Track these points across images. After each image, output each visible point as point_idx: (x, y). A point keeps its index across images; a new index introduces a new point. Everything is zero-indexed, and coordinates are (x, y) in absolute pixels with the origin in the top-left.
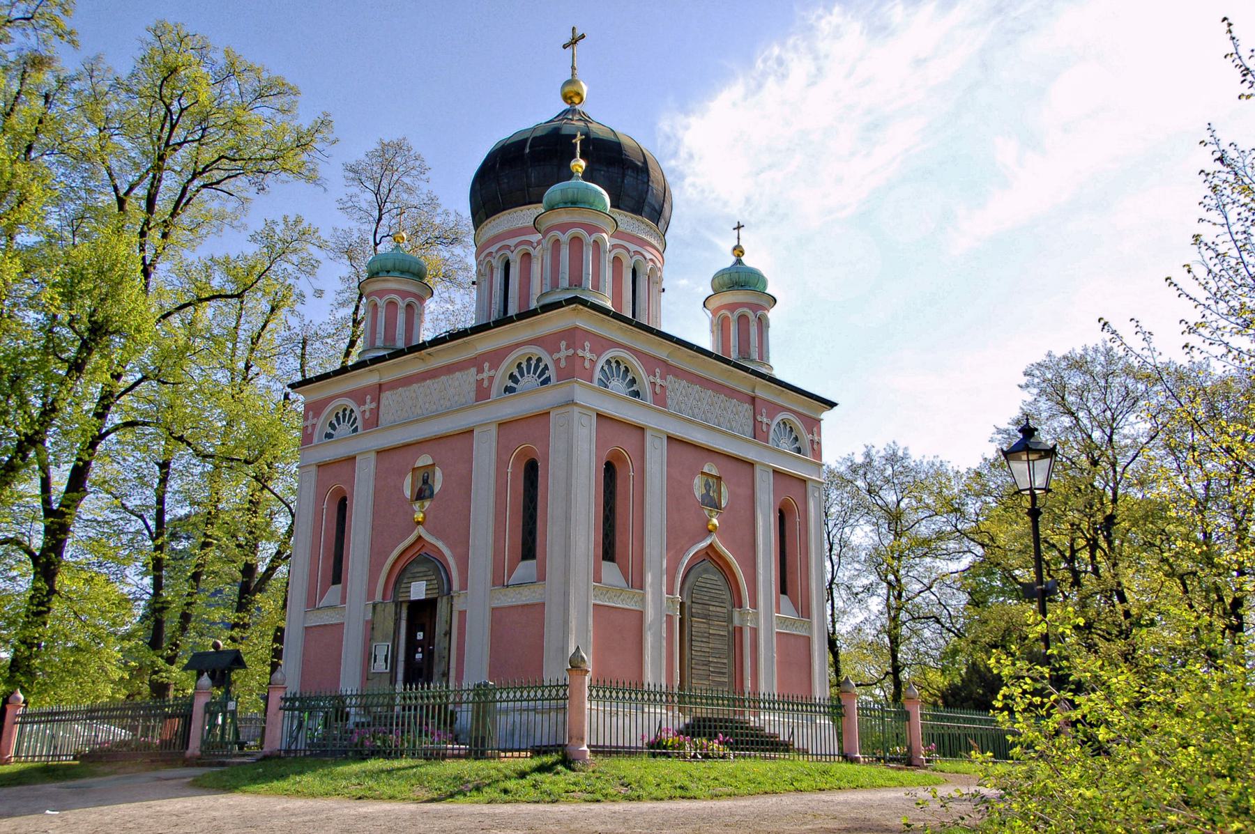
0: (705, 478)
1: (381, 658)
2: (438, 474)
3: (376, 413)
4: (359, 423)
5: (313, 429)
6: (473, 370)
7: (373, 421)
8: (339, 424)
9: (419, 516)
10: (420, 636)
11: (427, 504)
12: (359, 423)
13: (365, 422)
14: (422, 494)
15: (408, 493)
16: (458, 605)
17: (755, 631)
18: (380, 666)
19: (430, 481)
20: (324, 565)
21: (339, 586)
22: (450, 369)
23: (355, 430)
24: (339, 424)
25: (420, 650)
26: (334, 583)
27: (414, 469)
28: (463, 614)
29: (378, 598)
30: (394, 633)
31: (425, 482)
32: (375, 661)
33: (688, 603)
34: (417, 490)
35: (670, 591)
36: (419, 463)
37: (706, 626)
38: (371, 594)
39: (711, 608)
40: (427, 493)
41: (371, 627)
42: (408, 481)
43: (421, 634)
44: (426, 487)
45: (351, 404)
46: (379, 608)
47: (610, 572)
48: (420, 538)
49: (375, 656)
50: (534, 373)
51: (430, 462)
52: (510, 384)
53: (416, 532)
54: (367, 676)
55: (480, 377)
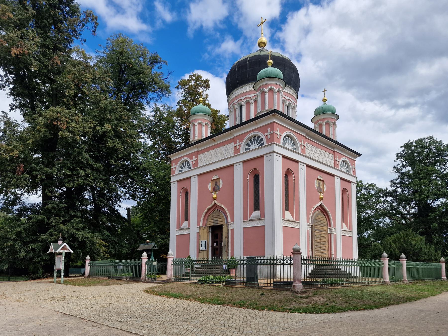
0: (318, 181)
1: (203, 245)
2: (221, 182)
3: (197, 161)
5: (175, 169)
8: (184, 167)
9: (215, 196)
11: (217, 193)
12: (191, 166)
13: (193, 164)
14: (215, 189)
15: (210, 189)
16: (231, 227)
17: (335, 235)
18: (203, 248)
19: (218, 184)
20: (182, 215)
21: (187, 222)
22: (223, 144)
23: (190, 168)
24: (184, 167)
26: (185, 221)
27: (212, 180)
28: (232, 230)
29: (201, 225)
30: (208, 236)
31: (216, 184)
32: (201, 247)
33: (314, 225)
34: (213, 188)
35: (308, 221)
36: (214, 178)
37: (319, 234)
38: (199, 224)
39: (321, 227)
40: (217, 188)
41: (199, 234)
42: (210, 185)
44: (217, 186)
45: (188, 159)
46: (202, 229)
47: (287, 213)
48: (215, 204)
49: (201, 245)
50: (257, 142)
51: (217, 177)
52: (247, 147)
53: (214, 202)
54: (199, 251)
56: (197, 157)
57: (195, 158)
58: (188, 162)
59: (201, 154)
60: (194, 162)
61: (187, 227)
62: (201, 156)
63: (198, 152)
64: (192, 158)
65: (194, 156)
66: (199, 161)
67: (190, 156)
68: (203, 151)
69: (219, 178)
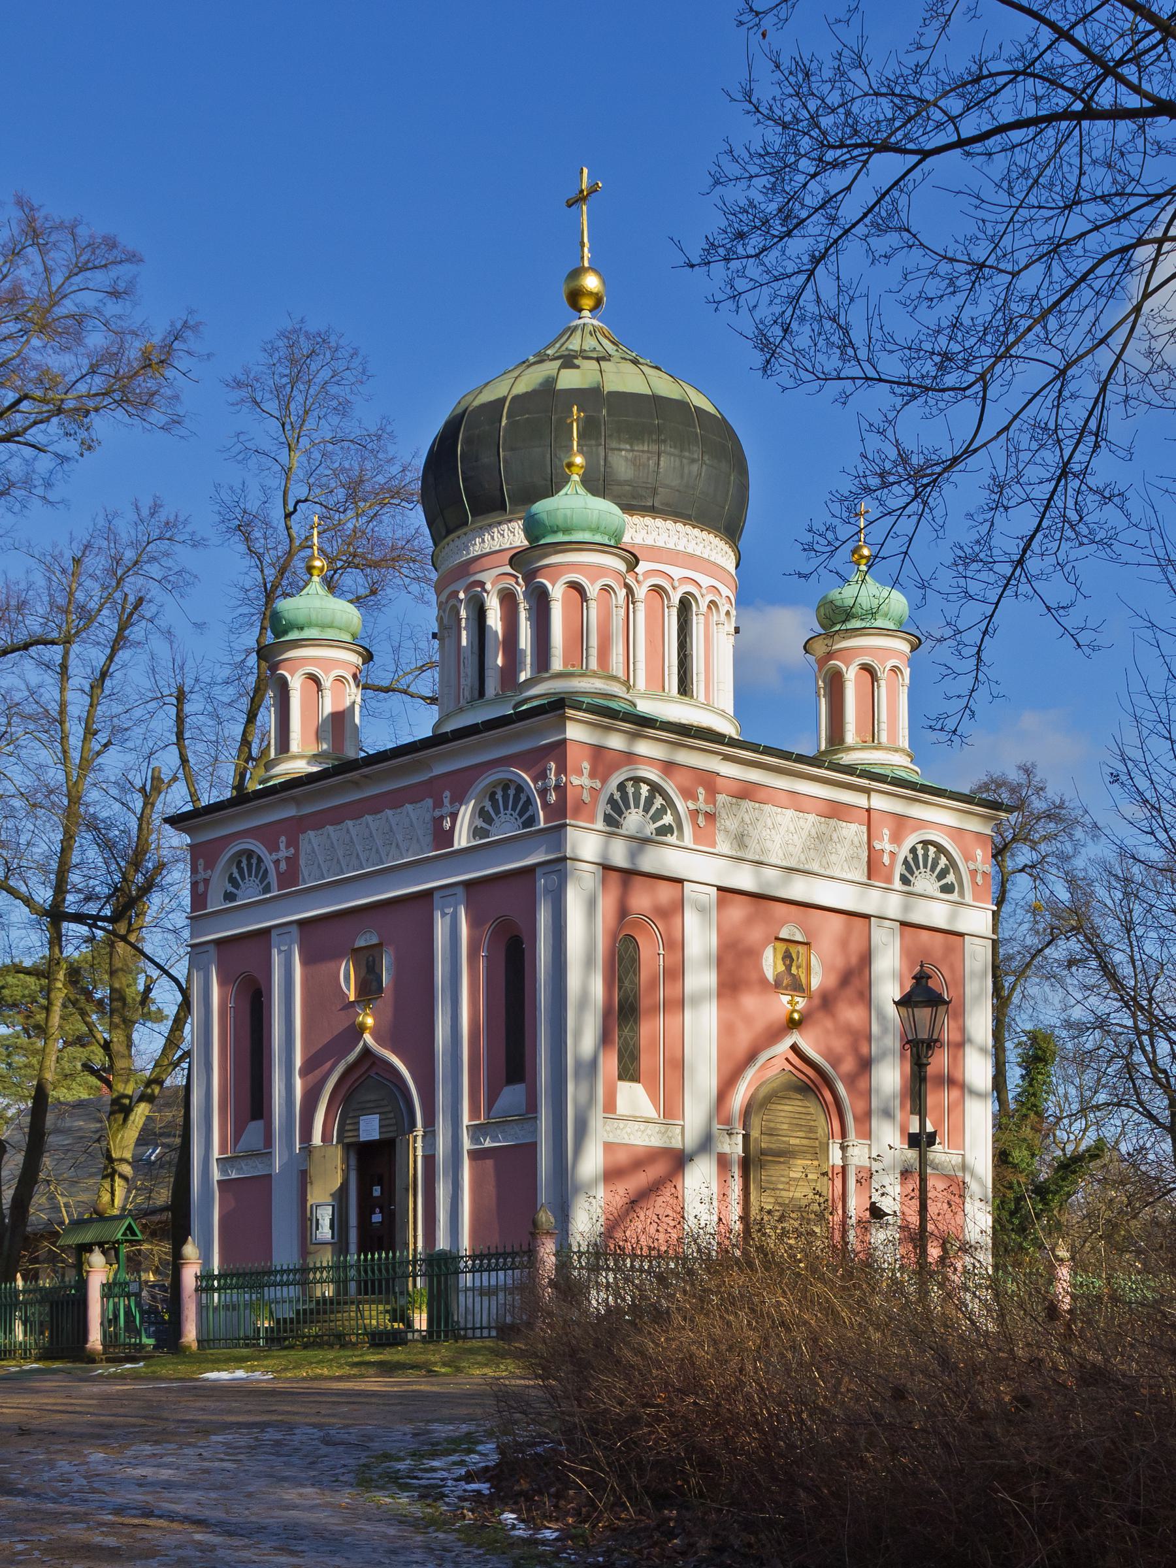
3: (293, 861)
4: (273, 877)
6: (429, 802)
7: (289, 876)
8: (243, 878)
10: (377, 1191)
12: (273, 877)
13: (279, 874)
24: (243, 878)
25: (377, 1210)
27: (356, 951)
32: (317, 1228)
36: (361, 943)
40: (374, 985)
43: (378, 1188)
49: (317, 1220)
51: (375, 941)
55: (437, 813)
56: (293, 843)
57: (287, 847)
58: (260, 860)
59: (311, 834)
60: (283, 866)
61: (261, 1145)
62: (311, 840)
63: (301, 819)
64: (273, 848)
65: (283, 839)
66: (302, 862)
67: (265, 833)
68: (318, 821)
69: (379, 945)
